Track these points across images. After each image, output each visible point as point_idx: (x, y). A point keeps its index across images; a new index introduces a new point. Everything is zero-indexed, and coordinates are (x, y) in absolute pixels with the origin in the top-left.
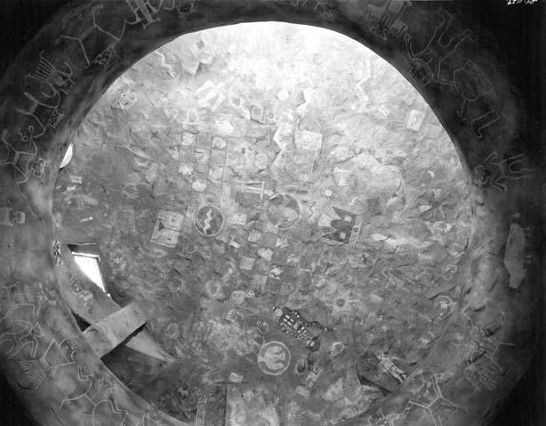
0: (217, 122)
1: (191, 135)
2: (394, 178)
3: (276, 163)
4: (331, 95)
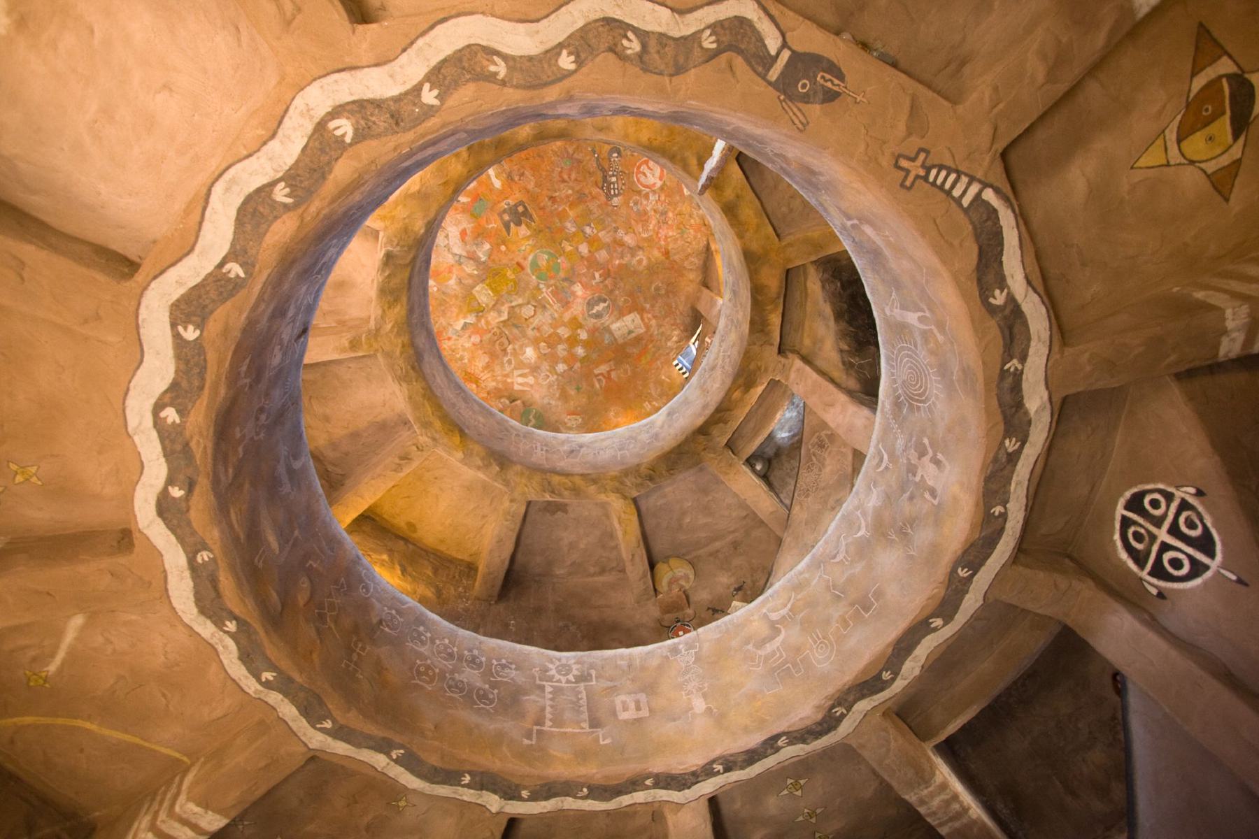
0: (533, 361)
3: (520, 301)
4: (443, 311)
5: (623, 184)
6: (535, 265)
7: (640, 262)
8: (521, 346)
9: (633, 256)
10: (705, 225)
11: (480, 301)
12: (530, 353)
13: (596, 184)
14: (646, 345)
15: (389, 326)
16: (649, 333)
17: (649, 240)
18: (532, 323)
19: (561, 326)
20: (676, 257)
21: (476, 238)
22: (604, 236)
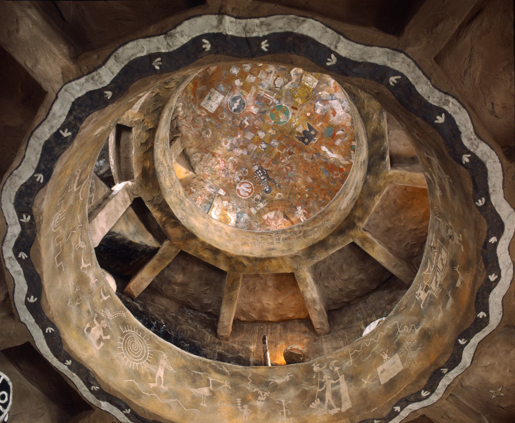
2: (347, 121)
3: (286, 87)
5: (256, 178)
6: (286, 113)
7: (226, 143)
9: (232, 144)
10: (202, 180)
11: (312, 76)
13: (271, 171)
14: (195, 96)
15: (375, 117)
16: (197, 104)
17: (227, 157)
19: (255, 81)
20: (207, 155)
22: (253, 147)
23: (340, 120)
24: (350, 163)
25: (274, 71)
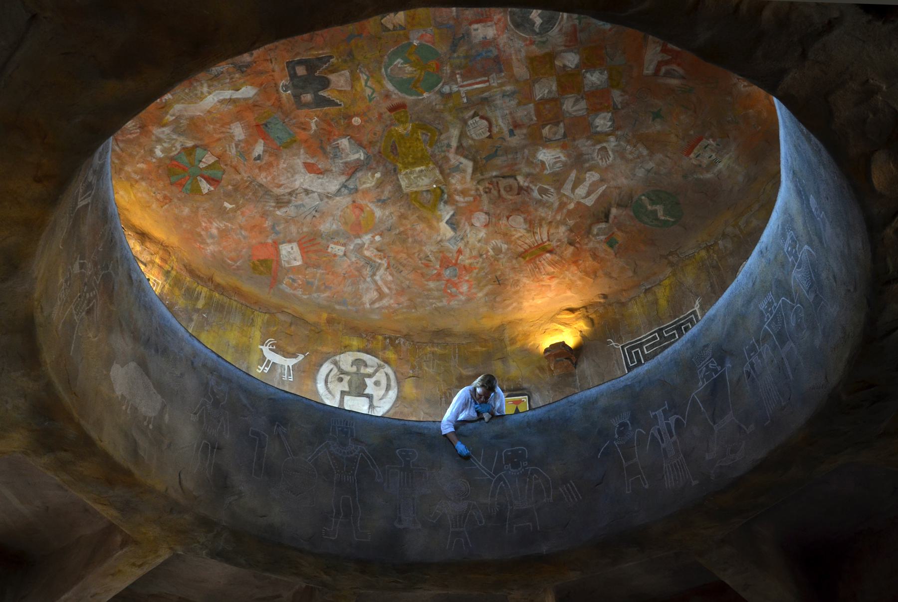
0: (563, 158)
1: (599, 129)
2: (273, 179)
3: (455, 133)
8: (529, 163)
11: (425, 188)
12: (547, 156)
18: (501, 131)
21: (325, 153)
23: (286, 169)
24: (165, 121)
25: (509, 139)
